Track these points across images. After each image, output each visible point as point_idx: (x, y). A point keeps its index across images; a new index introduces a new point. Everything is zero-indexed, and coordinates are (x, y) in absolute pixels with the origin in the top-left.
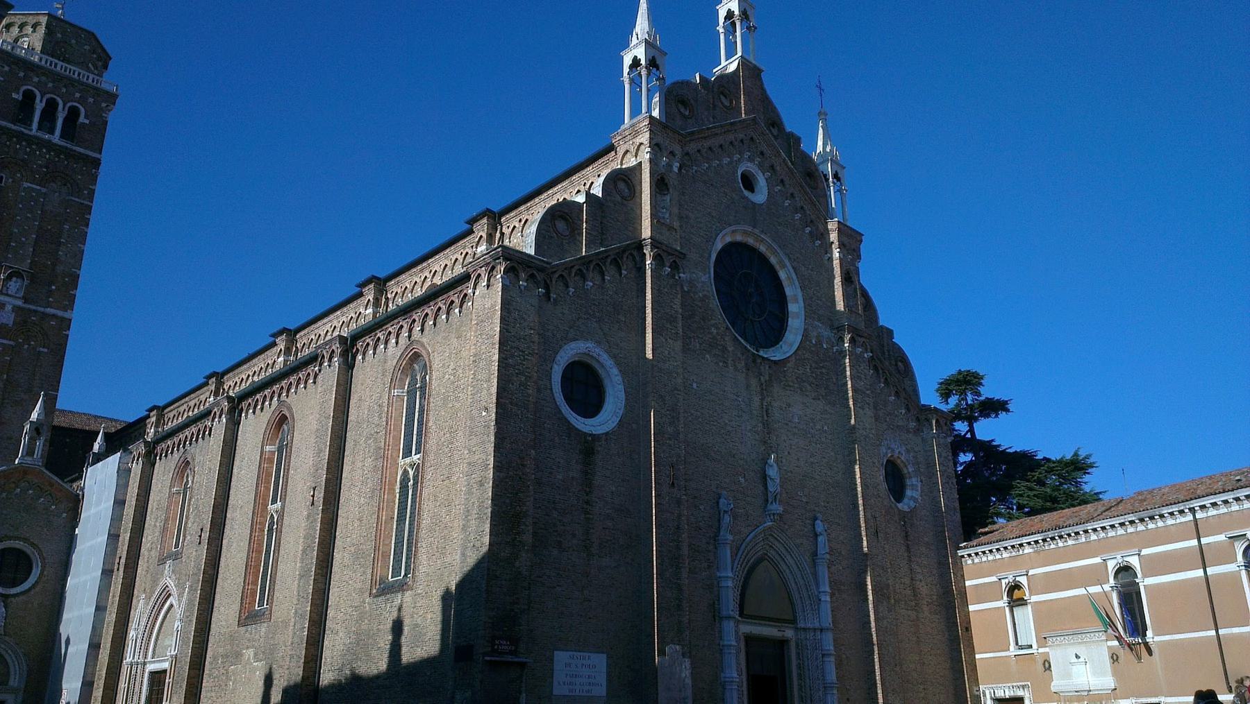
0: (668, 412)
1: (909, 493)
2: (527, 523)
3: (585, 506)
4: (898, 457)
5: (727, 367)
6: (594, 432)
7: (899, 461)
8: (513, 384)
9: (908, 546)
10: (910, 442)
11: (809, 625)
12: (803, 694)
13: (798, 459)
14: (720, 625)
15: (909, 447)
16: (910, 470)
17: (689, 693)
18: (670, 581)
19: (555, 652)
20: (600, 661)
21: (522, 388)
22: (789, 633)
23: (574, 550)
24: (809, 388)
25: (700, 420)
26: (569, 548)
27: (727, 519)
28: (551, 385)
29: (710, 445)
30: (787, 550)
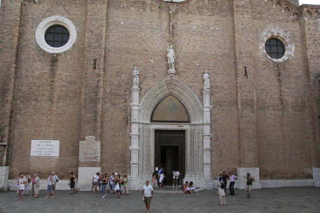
0: (95, 37)
1: (286, 53)
2: (10, 93)
3: (51, 83)
4: (277, 36)
5: (145, 11)
6: (56, 53)
7: (279, 38)
8: (5, 39)
9: (279, 79)
10: (288, 26)
11: (197, 123)
12: (192, 153)
13: (194, 46)
14: (131, 126)
15: (287, 29)
16: (287, 41)
17: (99, 155)
18: (90, 109)
19: (33, 141)
20: (56, 144)
21: (10, 40)
22: (186, 127)
23: (43, 101)
24: (206, 11)
25: (124, 37)
26: (41, 100)
27: (136, 80)
28: (35, 37)
29: (130, 48)
30: (183, 89)
